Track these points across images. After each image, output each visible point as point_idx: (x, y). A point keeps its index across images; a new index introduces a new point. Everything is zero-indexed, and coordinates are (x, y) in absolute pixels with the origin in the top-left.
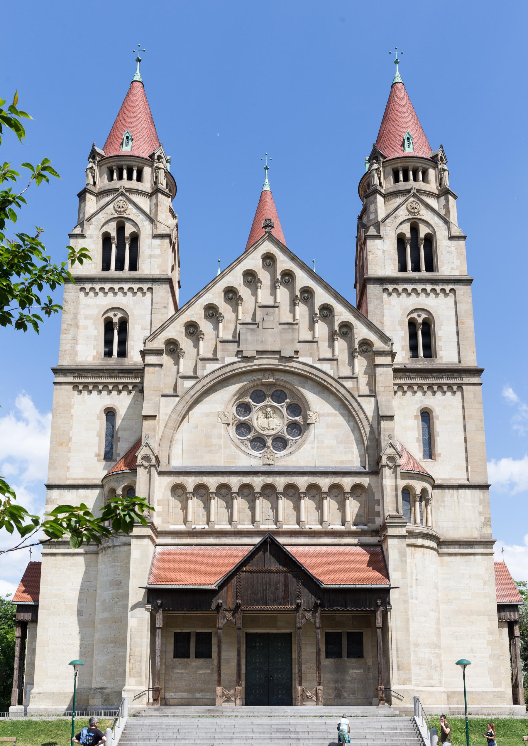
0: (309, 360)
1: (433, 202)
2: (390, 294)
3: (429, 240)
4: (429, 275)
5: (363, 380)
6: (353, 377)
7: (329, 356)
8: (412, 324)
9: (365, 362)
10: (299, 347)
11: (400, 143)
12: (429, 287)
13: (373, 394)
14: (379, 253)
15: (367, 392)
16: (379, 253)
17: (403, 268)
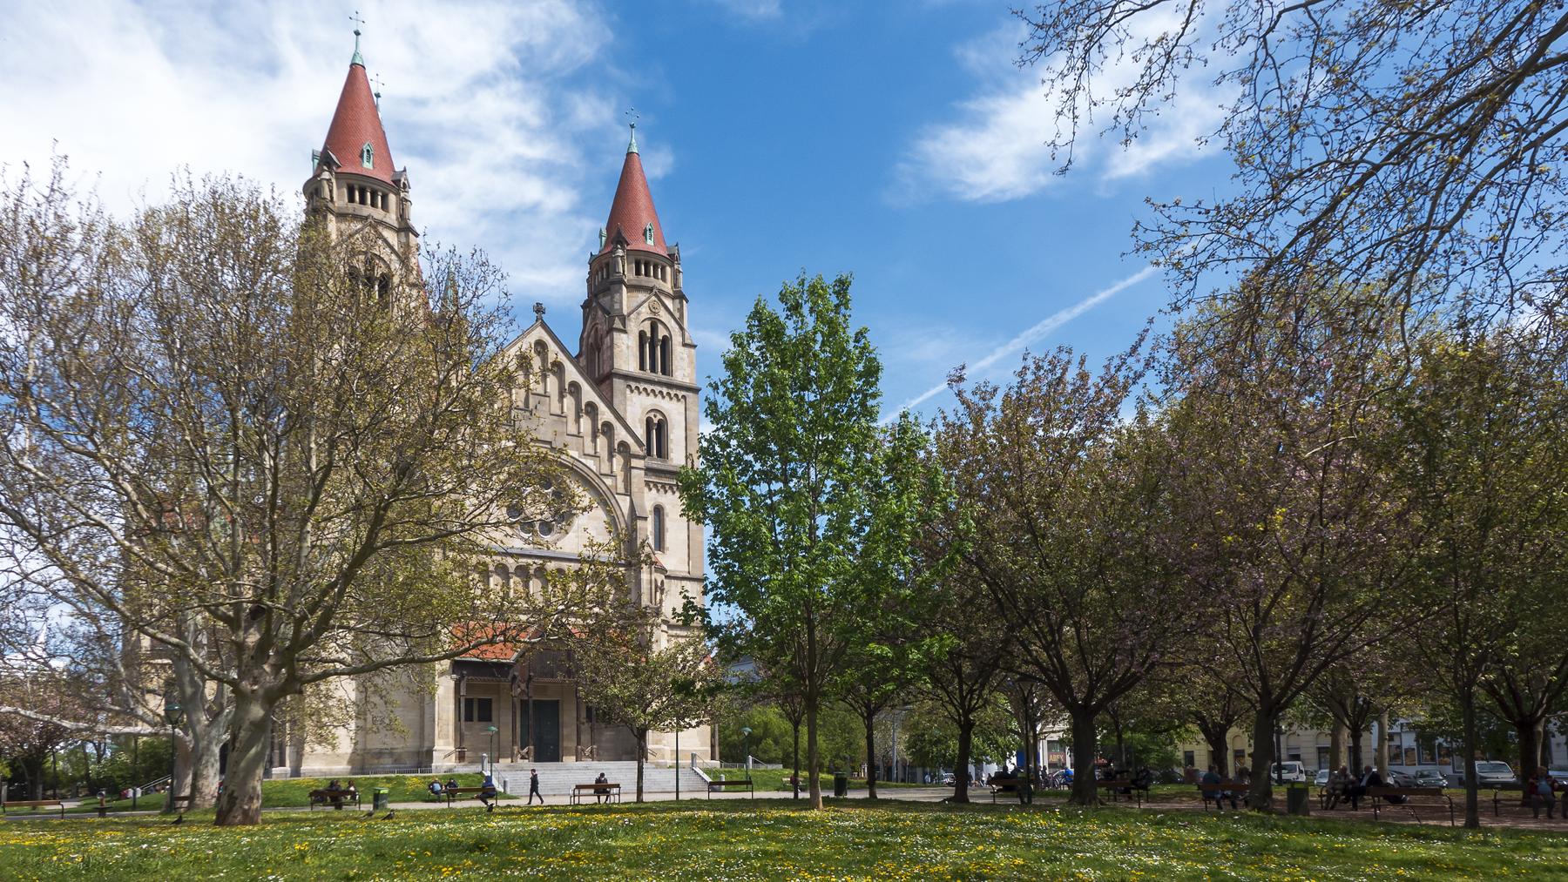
0: (575, 454)
1: (668, 303)
2: (632, 391)
3: (666, 342)
4: (664, 378)
5: (620, 478)
6: (611, 475)
7: (592, 453)
8: (649, 421)
9: (622, 461)
10: (568, 439)
11: (641, 232)
12: (665, 390)
13: (628, 492)
14: (624, 347)
15: (622, 491)
16: (624, 347)
17: (642, 367)
